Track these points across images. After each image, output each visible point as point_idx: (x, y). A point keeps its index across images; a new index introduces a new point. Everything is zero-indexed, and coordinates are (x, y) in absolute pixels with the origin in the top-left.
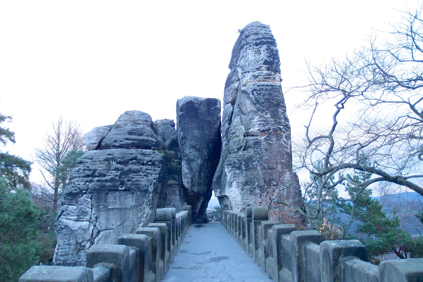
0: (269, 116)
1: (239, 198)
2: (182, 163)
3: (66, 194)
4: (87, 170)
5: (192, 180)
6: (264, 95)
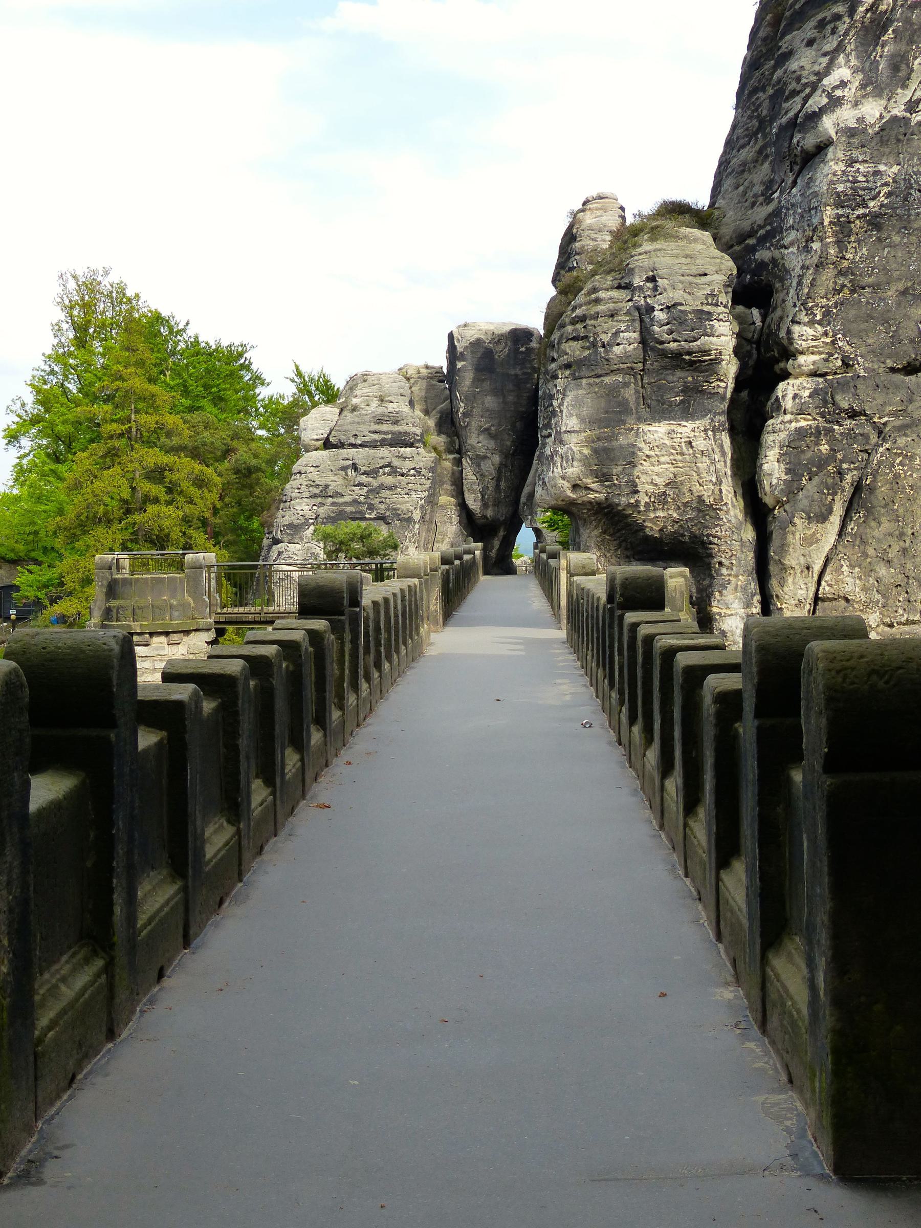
2: (464, 460)
3: (284, 526)
4: (311, 486)
5: (483, 496)
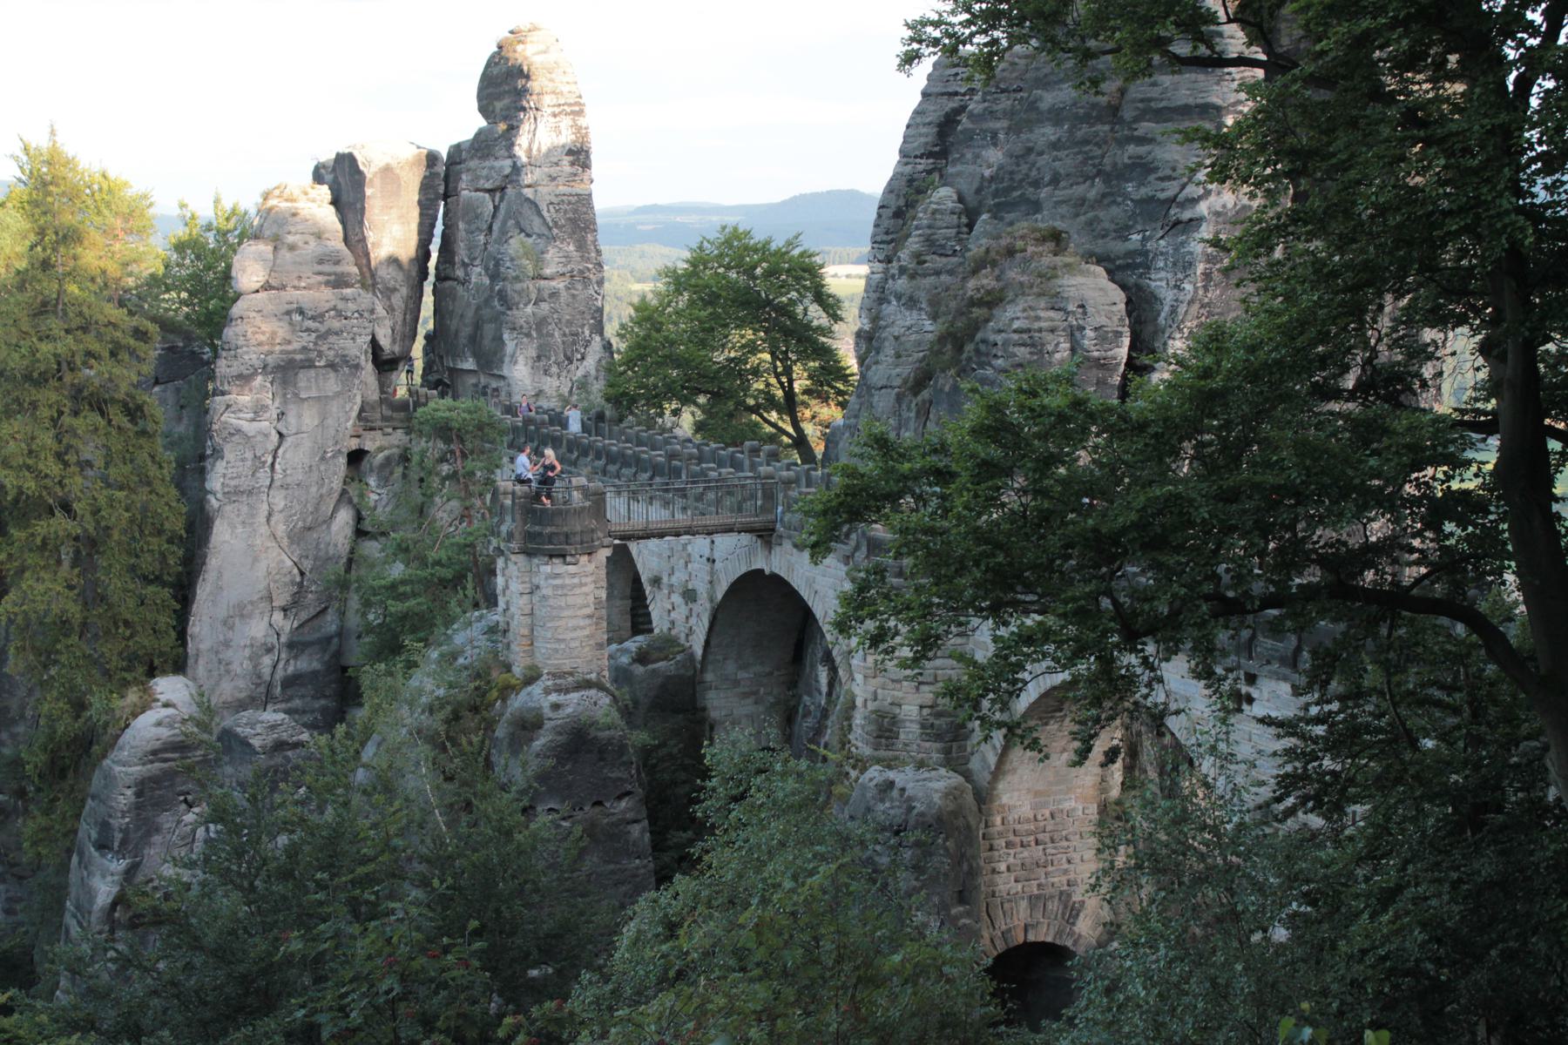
0: (572, 248)
1: (528, 382)
6: (566, 212)
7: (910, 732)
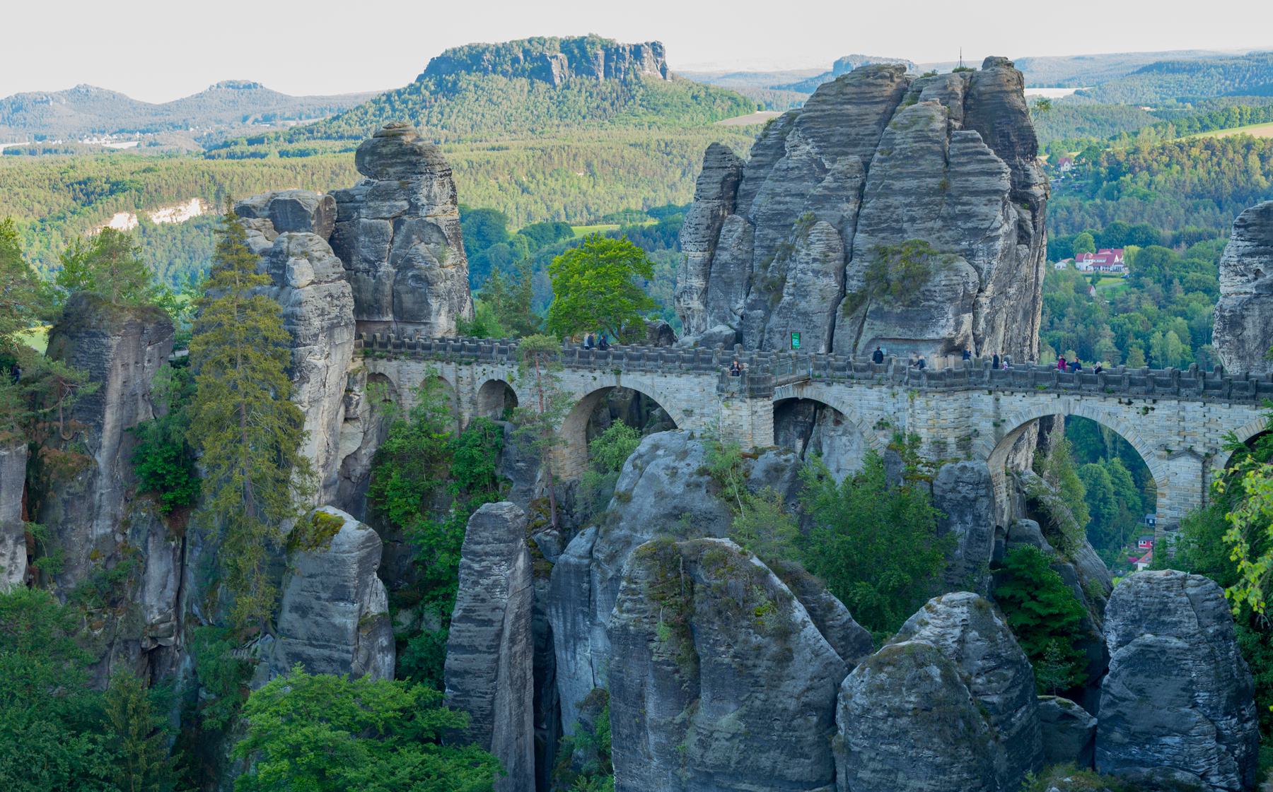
7: (952, 449)
